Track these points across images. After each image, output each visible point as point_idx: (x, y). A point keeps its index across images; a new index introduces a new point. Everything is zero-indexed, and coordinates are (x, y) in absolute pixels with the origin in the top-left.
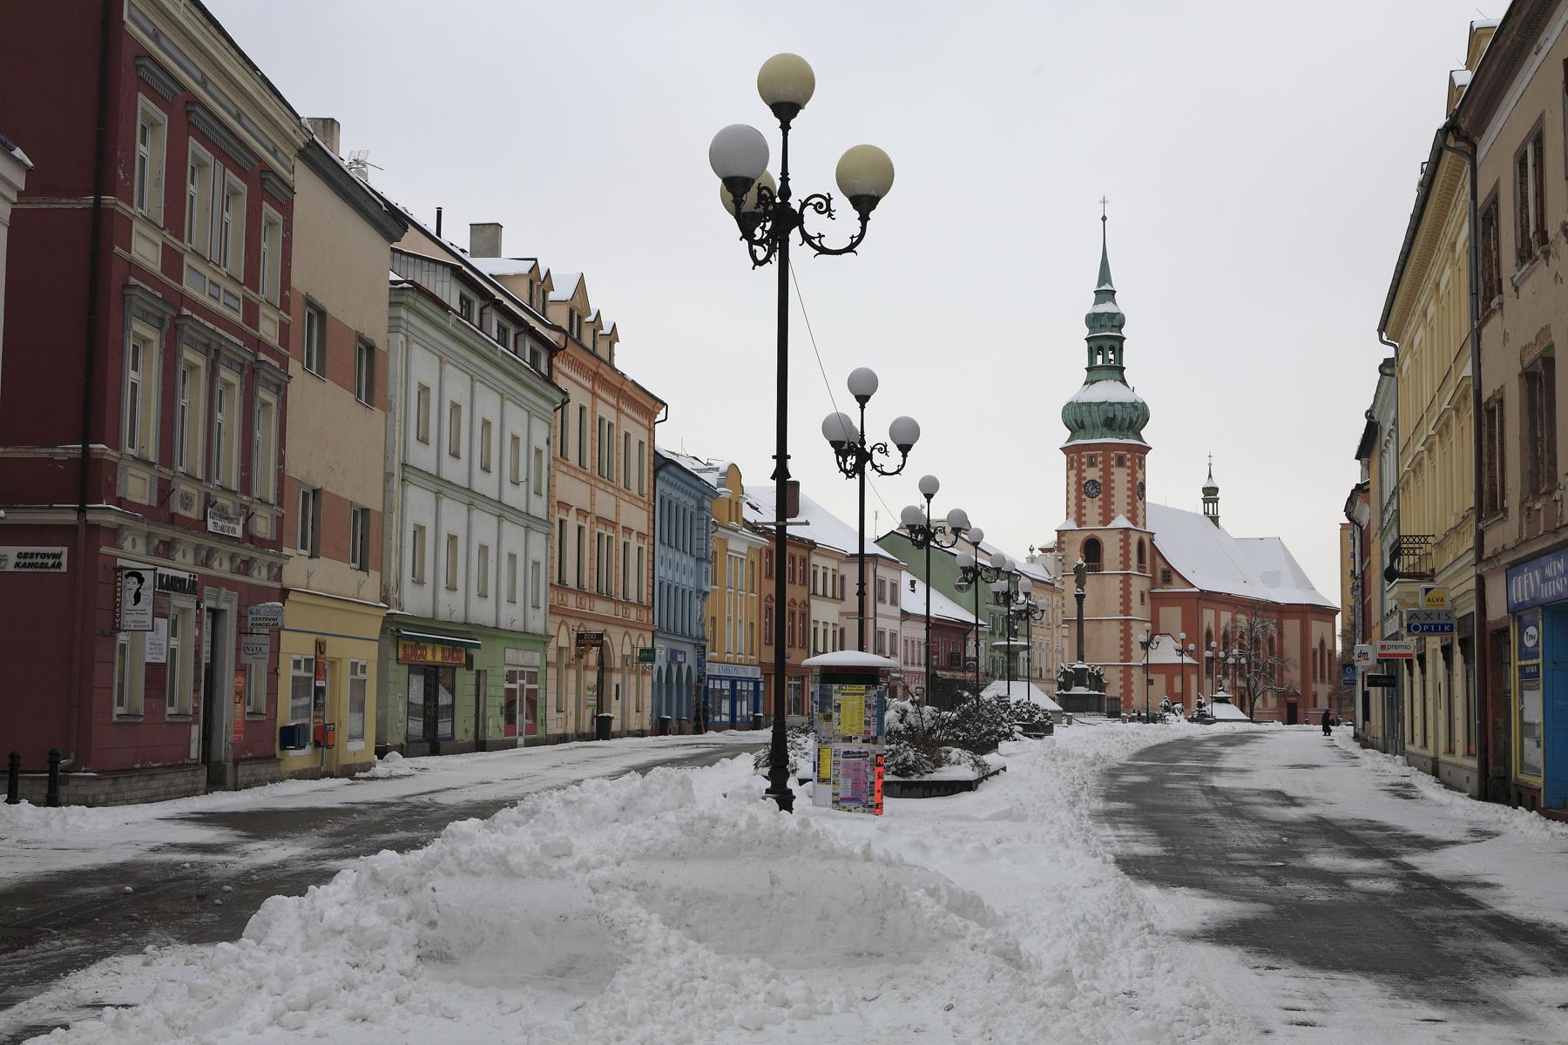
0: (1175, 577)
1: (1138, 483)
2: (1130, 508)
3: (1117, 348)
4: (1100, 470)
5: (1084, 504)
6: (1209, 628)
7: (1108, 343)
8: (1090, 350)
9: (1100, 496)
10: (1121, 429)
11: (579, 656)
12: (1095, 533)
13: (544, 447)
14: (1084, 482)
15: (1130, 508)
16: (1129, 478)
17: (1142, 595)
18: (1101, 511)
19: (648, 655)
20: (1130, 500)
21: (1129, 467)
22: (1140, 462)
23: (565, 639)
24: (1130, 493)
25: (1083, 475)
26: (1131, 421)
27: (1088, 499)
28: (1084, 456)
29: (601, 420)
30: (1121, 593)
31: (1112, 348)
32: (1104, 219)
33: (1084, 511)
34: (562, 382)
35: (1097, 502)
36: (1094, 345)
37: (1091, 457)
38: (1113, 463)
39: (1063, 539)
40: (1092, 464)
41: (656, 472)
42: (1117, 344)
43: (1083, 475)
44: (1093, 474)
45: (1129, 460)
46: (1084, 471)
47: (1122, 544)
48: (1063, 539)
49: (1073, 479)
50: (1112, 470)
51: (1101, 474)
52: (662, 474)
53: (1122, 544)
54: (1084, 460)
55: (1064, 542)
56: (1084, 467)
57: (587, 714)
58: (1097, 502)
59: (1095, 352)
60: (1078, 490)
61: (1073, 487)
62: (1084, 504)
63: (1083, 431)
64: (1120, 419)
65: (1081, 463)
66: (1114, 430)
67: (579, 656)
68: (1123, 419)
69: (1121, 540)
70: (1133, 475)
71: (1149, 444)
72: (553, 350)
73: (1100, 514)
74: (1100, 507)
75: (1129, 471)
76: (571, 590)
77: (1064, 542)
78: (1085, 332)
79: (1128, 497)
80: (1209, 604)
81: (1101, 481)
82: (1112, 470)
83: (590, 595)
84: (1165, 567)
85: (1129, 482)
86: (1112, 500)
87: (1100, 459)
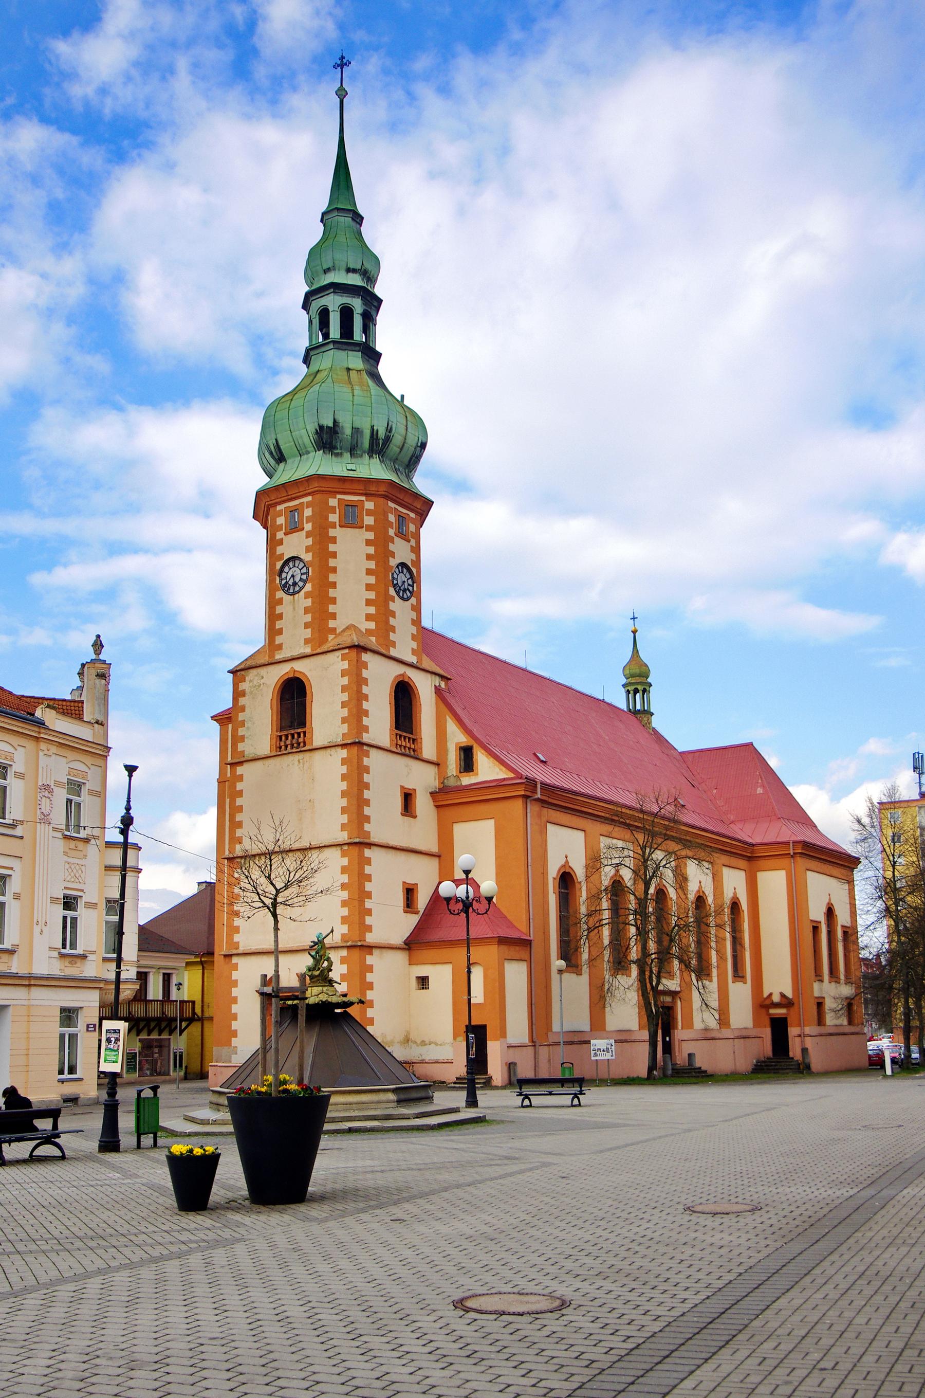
0: (481, 759)
1: (393, 562)
5: (279, 609)
7: (333, 302)
9: (308, 587)
10: (353, 450)
12: (300, 667)
14: (279, 565)
21: (369, 528)
22: (401, 519)
24: (372, 580)
25: (280, 550)
26: (374, 434)
27: (287, 598)
35: (302, 601)
37: (293, 510)
38: (334, 518)
39: (242, 686)
40: (294, 528)
42: (357, 305)
45: (370, 512)
46: (281, 542)
48: (242, 686)
50: (332, 532)
51: (310, 541)
54: (281, 521)
55: (243, 694)
56: (280, 535)
58: (302, 601)
63: (282, 465)
64: (348, 431)
66: (339, 455)
68: (356, 431)
73: (307, 626)
75: (371, 536)
77: (243, 694)
79: (369, 587)
81: (307, 557)
85: (369, 557)
87: (308, 512)
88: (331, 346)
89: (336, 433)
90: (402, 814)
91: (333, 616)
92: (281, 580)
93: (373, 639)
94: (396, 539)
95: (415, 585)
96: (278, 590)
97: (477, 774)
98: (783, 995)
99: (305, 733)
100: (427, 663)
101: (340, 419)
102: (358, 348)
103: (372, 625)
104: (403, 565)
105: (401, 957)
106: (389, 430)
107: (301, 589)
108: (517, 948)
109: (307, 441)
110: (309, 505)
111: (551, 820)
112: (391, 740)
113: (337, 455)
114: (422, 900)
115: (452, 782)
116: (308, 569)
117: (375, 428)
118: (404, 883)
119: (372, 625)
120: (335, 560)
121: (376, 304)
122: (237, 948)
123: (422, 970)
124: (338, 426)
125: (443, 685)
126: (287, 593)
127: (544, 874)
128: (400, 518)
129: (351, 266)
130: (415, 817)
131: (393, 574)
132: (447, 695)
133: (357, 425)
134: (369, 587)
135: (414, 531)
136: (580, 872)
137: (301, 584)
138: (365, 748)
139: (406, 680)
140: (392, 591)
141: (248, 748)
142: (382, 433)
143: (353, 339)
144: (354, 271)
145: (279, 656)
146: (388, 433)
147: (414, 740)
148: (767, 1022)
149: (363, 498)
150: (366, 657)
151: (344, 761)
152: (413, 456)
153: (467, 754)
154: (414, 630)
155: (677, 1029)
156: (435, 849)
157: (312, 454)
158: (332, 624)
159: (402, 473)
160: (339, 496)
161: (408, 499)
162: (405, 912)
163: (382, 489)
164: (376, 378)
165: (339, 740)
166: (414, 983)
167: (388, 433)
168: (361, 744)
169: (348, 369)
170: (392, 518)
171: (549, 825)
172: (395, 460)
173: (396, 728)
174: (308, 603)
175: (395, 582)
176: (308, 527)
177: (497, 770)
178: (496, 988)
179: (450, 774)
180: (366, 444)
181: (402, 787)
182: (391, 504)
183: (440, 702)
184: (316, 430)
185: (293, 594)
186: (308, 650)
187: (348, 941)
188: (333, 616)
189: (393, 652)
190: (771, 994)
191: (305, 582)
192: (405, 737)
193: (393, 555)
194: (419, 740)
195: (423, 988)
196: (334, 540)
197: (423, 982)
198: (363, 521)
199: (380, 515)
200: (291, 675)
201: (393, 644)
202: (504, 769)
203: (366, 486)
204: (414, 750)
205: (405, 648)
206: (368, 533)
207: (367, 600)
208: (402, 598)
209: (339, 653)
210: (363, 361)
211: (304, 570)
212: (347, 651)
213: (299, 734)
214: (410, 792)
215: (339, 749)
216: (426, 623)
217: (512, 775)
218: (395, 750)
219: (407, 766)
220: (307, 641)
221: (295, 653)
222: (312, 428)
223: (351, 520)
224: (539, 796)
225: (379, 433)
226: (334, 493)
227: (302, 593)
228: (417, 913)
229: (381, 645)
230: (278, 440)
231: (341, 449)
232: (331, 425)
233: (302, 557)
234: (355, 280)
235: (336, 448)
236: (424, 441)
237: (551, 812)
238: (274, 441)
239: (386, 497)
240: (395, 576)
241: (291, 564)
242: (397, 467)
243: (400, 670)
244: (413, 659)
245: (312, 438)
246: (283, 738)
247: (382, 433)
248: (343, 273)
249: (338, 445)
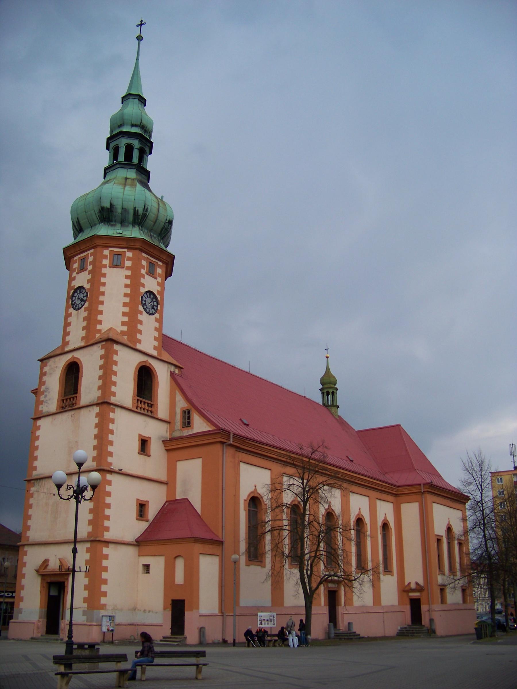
1: (143, 290)
5: (69, 320)
9: (87, 304)
10: (123, 222)
12: (77, 355)
21: (128, 268)
27: (75, 312)
35: (83, 313)
38: (106, 262)
40: (82, 269)
42: (136, 144)
46: (74, 279)
48: (46, 369)
50: (104, 271)
51: (90, 277)
58: (83, 313)
64: (119, 211)
75: (129, 273)
79: (125, 305)
82: (104, 271)
87: (91, 259)
88: (117, 166)
89: (112, 211)
90: (139, 453)
91: (100, 322)
92: (72, 301)
93: (126, 337)
94: (147, 276)
95: (159, 306)
96: (70, 308)
97: (193, 428)
98: (417, 584)
99: (76, 397)
100: (166, 356)
101: (115, 203)
102: (134, 167)
103: (125, 328)
104: (150, 292)
105: (132, 551)
106: (145, 209)
107: (83, 306)
108: (211, 546)
109: (94, 217)
110: (92, 254)
111: (244, 460)
112: (133, 403)
113: (112, 225)
114: (152, 512)
115: (177, 434)
116: (87, 293)
117: (137, 209)
118: (138, 499)
119: (125, 328)
120: (104, 287)
121: (149, 145)
122: (28, 540)
123: (146, 560)
124: (113, 207)
125: (177, 371)
126: (75, 309)
127: (236, 496)
128: (151, 264)
129: (134, 123)
130: (149, 456)
131: (142, 297)
132: (179, 379)
133: (125, 206)
134: (125, 305)
135: (161, 273)
136: (266, 498)
137: (83, 303)
138: (112, 406)
139: (148, 365)
140: (141, 308)
141: (45, 408)
142: (141, 211)
143: (132, 162)
144: (136, 126)
146: (145, 212)
147: (152, 406)
148: (408, 602)
149: (126, 250)
150: (116, 347)
152: (163, 228)
153: (187, 415)
154: (156, 334)
155: (341, 605)
156: (163, 478)
157: (97, 226)
158: (99, 327)
159: (155, 238)
160: (110, 249)
161: (156, 252)
162: (137, 519)
163: (138, 245)
165: (96, 401)
166: (141, 568)
167: (145, 212)
170: (144, 263)
171: (242, 464)
172: (151, 230)
173: (138, 396)
175: (144, 302)
176: (90, 268)
177: (205, 424)
179: (176, 429)
180: (131, 218)
181: (140, 435)
182: (144, 254)
183: (173, 382)
184: (100, 210)
185: (78, 310)
186: (83, 344)
187: (91, 537)
188: (100, 322)
189: (139, 346)
190: (409, 583)
191: (85, 301)
192: (145, 403)
193: (143, 285)
194: (155, 406)
195: (147, 573)
197: (147, 568)
198: (124, 263)
199: (136, 262)
200: (72, 361)
201: (140, 341)
202: (209, 424)
204: (151, 412)
206: (127, 271)
207: (123, 312)
208: (149, 313)
209: (100, 345)
210: (136, 174)
211: (85, 295)
212: (104, 343)
213: (73, 398)
214: (146, 439)
215: (95, 407)
216: (166, 331)
217: (214, 428)
218: (136, 410)
219: (145, 421)
221: (77, 346)
222: (97, 209)
223: (116, 264)
224: (231, 442)
225: (139, 212)
226: (107, 247)
227: (83, 308)
228: (147, 521)
229: (130, 341)
230: (79, 218)
231: (115, 222)
232: (108, 206)
233: (85, 286)
235: (112, 221)
236: (171, 219)
237: (244, 455)
238: (77, 220)
239: (142, 251)
240: (144, 298)
241: (78, 291)
242: (152, 234)
243: (143, 358)
244: (155, 353)
245: (96, 213)
246: (65, 401)
247: (141, 211)
248: (130, 127)
249: (114, 219)
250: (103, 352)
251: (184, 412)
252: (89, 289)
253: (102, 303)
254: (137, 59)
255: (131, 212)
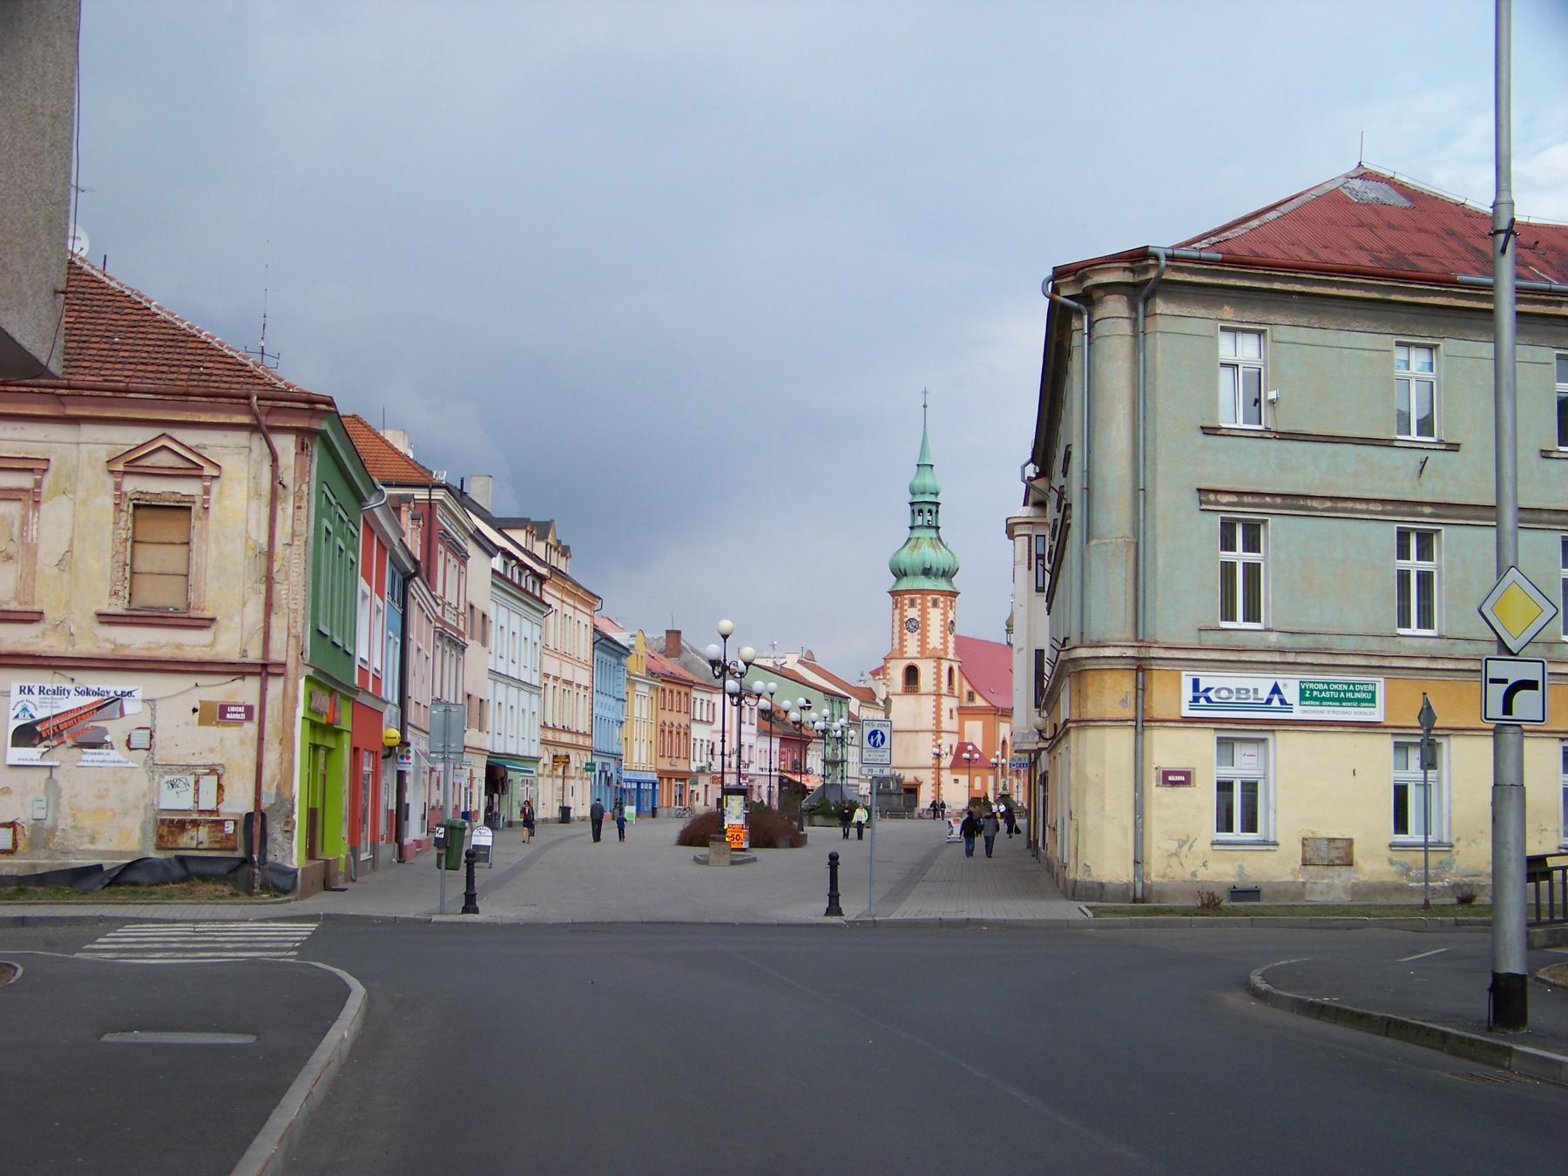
0: (977, 698)
1: (949, 621)
2: (942, 641)
3: (934, 511)
4: (919, 610)
5: (905, 637)
6: (1004, 737)
8: (913, 511)
9: (919, 631)
11: (554, 768)
12: (917, 663)
13: (538, 641)
14: (906, 620)
15: (942, 641)
16: (942, 617)
17: (951, 711)
18: (919, 643)
19: (590, 767)
20: (942, 635)
21: (942, 608)
23: (547, 759)
24: (942, 629)
25: (905, 613)
26: (944, 571)
28: (906, 599)
29: (565, 615)
30: (934, 709)
31: (930, 511)
32: (925, 406)
33: (905, 643)
34: (547, 599)
35: (916, 636)
36: (917, 508)
38: (929, 604)
40: (912, 604)
41: (594, 643)
42: (933, 508)
43: (905, 613)
44: (913, 613)
46: (906, 610)
47: (935, 670)
48: (888, 665)
49: (897, 617)
50: (928, 610)
51: (920, 613)
52: (596, 645)
53: (935, 670)
56: (906, 607)
57: (557, 805)
58: (916, 636)
59: (916, 514)
60: (900, 626)
61: (897, 623)
62: (905, 637)
63: (905, 578)
64: (935, 569)
65: (903, 604)
67: (554, 768)
68: (938, 569)
69: (934, 667)
70: (945, 614)
71: (959, 590)
72: (542, 579)
73: (918, 646)
74: (918, 640)
75: (942, 611)
76: (550, 728)
78: (910, 498)
79: (941, 632)
80: (1004, 719)
81: (919, 619)
83: (559, 730)
84: (970, 689)
86: (928, 634)
87: (919, 601)
91: (929, 643)
93: (942, 652)
103: (942, 647)
105: (948, 772)
115: (965, 705)
119: (942, 647)
123: (956, 777)
134: (941, 632)
145: (905, 656)
150: (942, 661)
151: (934, 701)
156: (956, 729)
158: (928, 646)
163: (947, 593)
164: (939, 539)
168: (940, 695)
169: (931, 538)
170: (949, 603)
174: (919, 637)
178: (984, 784)
186: (919, 656)
188: (929, 643)
189: (949, 657)
196: (929, 613)
199: (945, 602)
203: (942, 593)
205: (951, 656)
220: (918, 652)
232: (929, 567)
234: (932, 498)
250: (935, 664)
251: (970, 693)
252: (921, 622)
253: (929, 631)
254: (925, 426)
255: (942, 570)
